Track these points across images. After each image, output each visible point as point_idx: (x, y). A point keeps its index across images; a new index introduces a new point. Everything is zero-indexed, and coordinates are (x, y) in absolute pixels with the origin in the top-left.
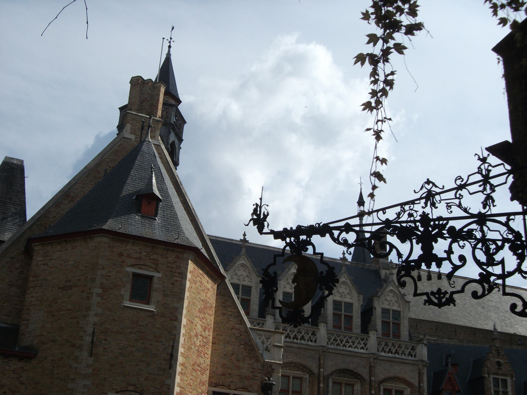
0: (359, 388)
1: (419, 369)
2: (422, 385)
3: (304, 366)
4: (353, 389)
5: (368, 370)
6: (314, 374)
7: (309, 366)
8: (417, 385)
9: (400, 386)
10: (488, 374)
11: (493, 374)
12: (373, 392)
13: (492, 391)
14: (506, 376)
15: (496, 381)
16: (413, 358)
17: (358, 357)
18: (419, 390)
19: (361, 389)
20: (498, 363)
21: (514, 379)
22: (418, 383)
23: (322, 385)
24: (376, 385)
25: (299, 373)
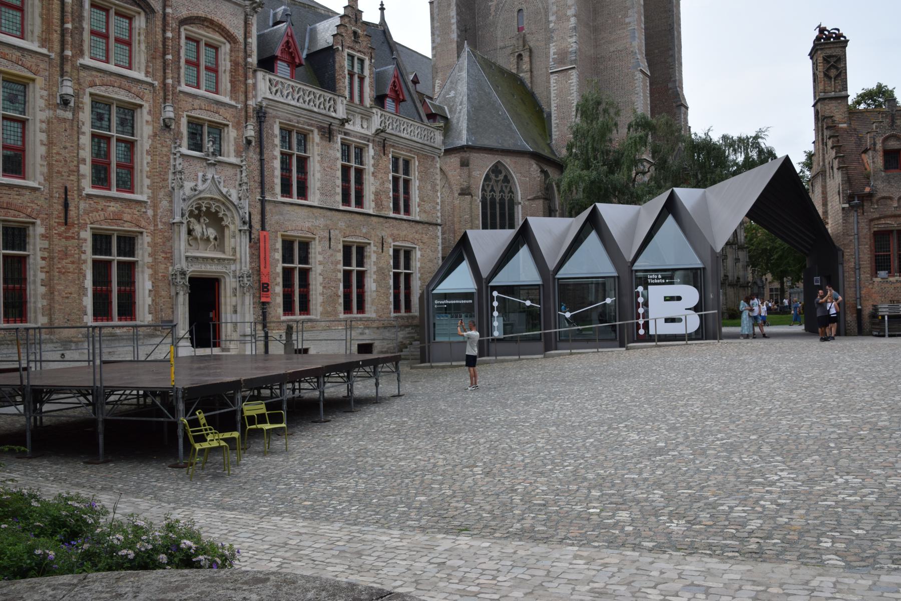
0: (143, 25)
1: (246, 15)
2: (249, 40)
4: (130, 24)
8: (241, 38)
10: (342, 46)
11: (349, 48)
12: (169, 34)
13: (346, 72)
14: (365, 54)
15: (351, 57)
19: (147, 26)
20: (355, 33)
22: (243, 36)
24: (174, 25)
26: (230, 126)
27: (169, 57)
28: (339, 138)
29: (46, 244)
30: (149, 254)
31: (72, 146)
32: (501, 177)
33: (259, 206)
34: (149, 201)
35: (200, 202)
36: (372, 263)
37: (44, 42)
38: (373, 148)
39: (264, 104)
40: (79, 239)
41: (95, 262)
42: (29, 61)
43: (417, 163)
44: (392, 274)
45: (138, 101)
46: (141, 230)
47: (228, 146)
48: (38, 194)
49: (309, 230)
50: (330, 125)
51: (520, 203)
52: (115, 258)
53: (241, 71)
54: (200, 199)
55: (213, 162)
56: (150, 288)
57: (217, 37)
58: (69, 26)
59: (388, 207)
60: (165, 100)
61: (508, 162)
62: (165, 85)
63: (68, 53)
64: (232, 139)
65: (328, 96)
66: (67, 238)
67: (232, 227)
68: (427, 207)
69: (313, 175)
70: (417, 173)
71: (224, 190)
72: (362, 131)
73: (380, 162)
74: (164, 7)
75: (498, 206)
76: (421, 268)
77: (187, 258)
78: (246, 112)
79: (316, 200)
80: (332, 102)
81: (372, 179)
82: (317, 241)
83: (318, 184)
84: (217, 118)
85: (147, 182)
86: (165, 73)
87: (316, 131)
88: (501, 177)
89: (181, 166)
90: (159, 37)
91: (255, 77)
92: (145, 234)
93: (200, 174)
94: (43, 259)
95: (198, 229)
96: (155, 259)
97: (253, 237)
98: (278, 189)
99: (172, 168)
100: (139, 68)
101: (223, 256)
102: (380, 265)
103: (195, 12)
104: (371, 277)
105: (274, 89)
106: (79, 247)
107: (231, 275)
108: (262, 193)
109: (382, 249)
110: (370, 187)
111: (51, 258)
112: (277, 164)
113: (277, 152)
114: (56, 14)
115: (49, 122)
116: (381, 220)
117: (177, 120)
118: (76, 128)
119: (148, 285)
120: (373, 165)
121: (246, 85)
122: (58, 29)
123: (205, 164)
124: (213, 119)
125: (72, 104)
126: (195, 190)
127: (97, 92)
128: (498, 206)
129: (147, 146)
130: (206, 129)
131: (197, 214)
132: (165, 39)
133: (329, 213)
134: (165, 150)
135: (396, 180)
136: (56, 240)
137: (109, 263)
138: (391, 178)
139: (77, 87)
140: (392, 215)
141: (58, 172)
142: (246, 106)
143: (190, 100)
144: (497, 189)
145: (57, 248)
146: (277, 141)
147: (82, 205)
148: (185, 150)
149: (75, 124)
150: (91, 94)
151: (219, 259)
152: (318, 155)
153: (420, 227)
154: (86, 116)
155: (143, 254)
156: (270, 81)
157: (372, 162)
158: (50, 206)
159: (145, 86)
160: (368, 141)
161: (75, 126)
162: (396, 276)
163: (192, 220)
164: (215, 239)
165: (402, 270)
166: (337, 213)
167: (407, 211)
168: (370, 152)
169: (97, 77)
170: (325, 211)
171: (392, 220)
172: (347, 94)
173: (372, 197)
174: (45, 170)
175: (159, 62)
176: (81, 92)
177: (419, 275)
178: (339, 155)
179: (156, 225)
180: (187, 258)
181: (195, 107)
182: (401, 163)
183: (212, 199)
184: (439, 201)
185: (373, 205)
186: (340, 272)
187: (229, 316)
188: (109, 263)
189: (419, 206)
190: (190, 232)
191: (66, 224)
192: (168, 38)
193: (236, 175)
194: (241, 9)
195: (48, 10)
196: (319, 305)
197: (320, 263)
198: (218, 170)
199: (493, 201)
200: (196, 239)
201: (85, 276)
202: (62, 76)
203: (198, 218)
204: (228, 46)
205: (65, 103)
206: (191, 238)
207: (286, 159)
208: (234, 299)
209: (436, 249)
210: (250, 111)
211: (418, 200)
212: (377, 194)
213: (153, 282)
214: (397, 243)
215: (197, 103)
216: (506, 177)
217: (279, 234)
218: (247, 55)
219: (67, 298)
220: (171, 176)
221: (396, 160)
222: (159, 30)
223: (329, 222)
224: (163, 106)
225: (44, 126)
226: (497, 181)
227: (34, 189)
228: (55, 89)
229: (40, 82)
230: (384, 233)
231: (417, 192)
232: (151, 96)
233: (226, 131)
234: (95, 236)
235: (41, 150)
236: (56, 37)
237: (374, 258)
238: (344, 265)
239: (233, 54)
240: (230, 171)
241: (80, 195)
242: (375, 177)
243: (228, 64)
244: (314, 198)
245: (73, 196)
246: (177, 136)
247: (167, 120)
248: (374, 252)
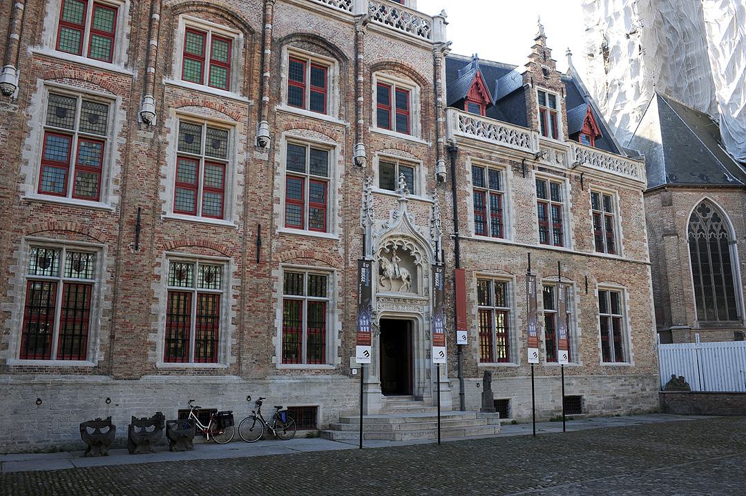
0: (337, 73)
1: (435, 58)
2: (439, 81)
3: (234, 16)
5: (352, 43)
6: (253, 32)
7: (244, 17)
8: (430, 80)
9: (405, 82)
11: (539, 84)
12: (361, 78)
14: (556, 90)
15: (542, 94)
16: (426, 39)
17: (335, 18)
18: (435, 90)
20: (544, 70)
21: (565, 96)
23: (268, 52)
25: (225, 29)
26: (422, 164)
27: (361, 99)
28: (533, 173)
29: (237, 282)
30: (340, 294)
31: (266, 186)
32: (710, 215)
33: (452, 243)
34: (340, 239)
35: (391, 240)
36: (576, 305)
37: (246, 91)
38: (570, 183)
39: (455, 141)
40: (270, 277)
41: (285, 301)
43: (619, 198)
44: (598, 317)
46: (332, 268)
47: (420, 184)
48: (233, 232)
49: (506, 269)
50: (524, 160)
51: (735, 242)
52: (306, 298)
53: (431, 111)
54: (391, 237)
55: (404, 199)
56: (341, 329)
57: (408, 80)
58: (268, 74)
59: (591, 245)
60: (357, 139)
61: (716, 198)
62: (357, 125)
63: (266, 99)
64: (423, 176)
65: (520, 130)
66: (258, 276)
67: (424, 265)
68: (634, 244)
69: (508, 212)
70: (619, 208)
71: (416, 228)
72: (558, 166)
73: (579, 197)
74: (357, 53)
75: (709, 246)
76: (632, 311)
77: (378, 298)
78: (438, 150)
79: (513, 238)
80: (524, 137)
81: (571, 214)
82: (515, 281)
83: (513, 222)
84: (409, 157)
85: (339, 220)
86: (357, 114)
87: (509, 167)
88: (710, 215)
89: (372, 204)
90: (352, 82)
91: (445, 115)
92: (336, 273)
93: (391, 212)
94: (235, 297)
95: (390, 268)
96: (346, 298)
97: (446, 275)
98: (471, 226)
99: (363, 205)
100: (333, 112)
101: (413, 296)
102: (584, 308)
103: (385, 58)
104: (575, 321)
105: (465, 126)
106: (270, 285)
107: (424, 317)
108: (456, 230)
109: (587, 290)
110: (570, 224)
111: (242, 296)
112: (470, 201)
113: (470, 189)
114: (257, 66)
115: (247, 164)
116: (584, 258)
117: (369, 161)
118: (271, 169)
119: (338, 326)
120: (571, 201)
121: (437, 123)
122: (258, 78)
123: (396, 202)
124: (404, 158)
125: (268, 146)
126: (387, 228)
127: (293, 135)
128: (709, 246)
129: (339, 185)
130: (397, 168)
131: (391, 251)
132: (357, 82)
134: (357, 187)
135: (597, 217)
136: (248, 279)
137: (301, 301)
138: (591, 214)
139: (273, 130)
140: (595, 253)
141: (253, 211)
142: (437, 143)
143: (382, 140)
144: (706, 228)
145: (248, 286)
146: (469, 177)
147: (275, 243)
148: (375, 187)
149: (271, 164)
151: (411, 300)
152: (513, 191)
153: (626, 266)
154: (282, 157)
155: (334, 293)
157: (570, 197)
158: (244, 244)
159: (339, 128)
160: (565, 176)
161: (271, 166)
162: (604, 320)
163: (384, 258)
164: (408, 279)
165: (609, 314)
167: (611, 250)
168: (567, 189)
169: (292, 120)
171: (595, 259)
172: (539, 128)
173: (572, 234)
174: (241, 209)
175: (351, 106)
176: (277, 135)
177: (629, 319)
178: (534, 190)
179: (347, 264)
180: (378, 298)
181: (386, 146)
182: (601, 198)
183: (403, 237)
184: (646, 237)
185: (574, 242)
187: (421, 360)
188: (301, 301)
189: (623, 244)
190: (382, 272)
191: (258, 262)
192: (360, 82)
193: (428, 212)
194: (430, 54)
195: (250, 62)
196: (519, 351)
198: (410, 208)
199: (702, 239)
200: (388, 278)
201: (275, 316)
202: (260, 120)
203: (390, 256)
204: (418, 88)
206: (383, 278)
207: (479, 196)
208: (427, 342)
209: (647, 290)
210: (442, 147)
211: (622, 236)
212: (577, 230)
213: (343, 323)
214: (602, 284)
216: (715, 214)
218: (437, 94)
219: (256, 337)
220: (362, 214)
221: (595, 196)
222: (351, 76)
224: (355, 146)
225: (242, 168)
226: (706, 221)
227: (230, 228)
228: (253, 132)
229: (240, 127)
230: (587, 273)
231: (621, 228)
232: (343, 137)
233: (417, 170)
234: (287, 274)
235: (239, 191)
236: (255, 86)
237: (577, 299)
238: (545, 309)
239: (423, 95)
240: (422, 209)
241: (273, 234)
242: (574, 213)
243: (419, 106)
244: (511, 236)
245: (266, 235)
246: (371, 172)
247: (358, 159)
248: (578, 293)
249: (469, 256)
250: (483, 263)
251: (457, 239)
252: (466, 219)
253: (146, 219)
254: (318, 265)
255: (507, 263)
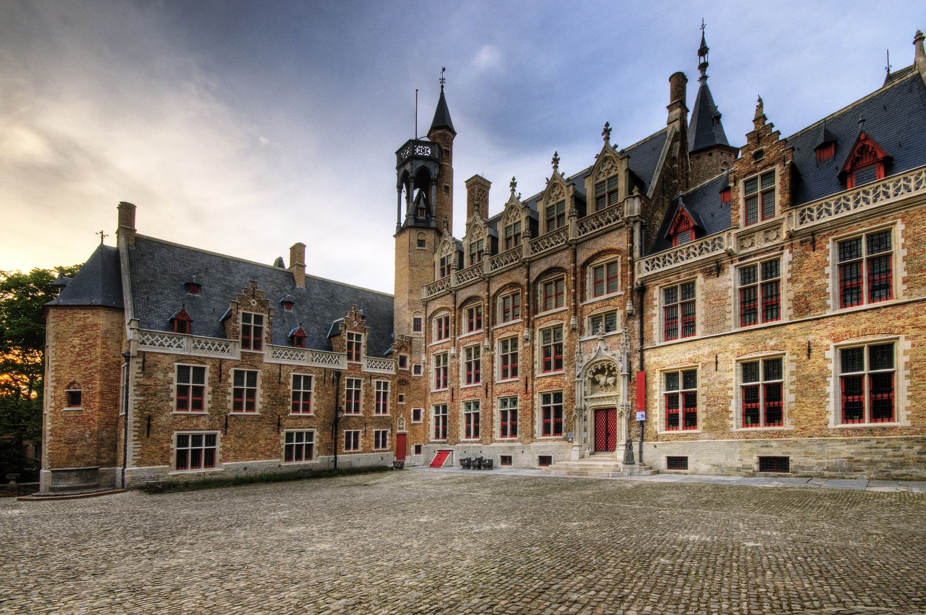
33: (638, 355)
42: (516, 327)
45: (561, 322)
49: (690, 359)
54: (596, 362)
57: (612, 256)
83: (703, 319)
84: (609, 309)
133: (717, 340)
150: (540, 330)
156: (647, 262)
166: (727, 337)
170: (710, 340)
186: (732, 389)
197: (703, 386)
205: (527, 340)
215: (594, 307)
217: (657, 371)
223: (716, 348)
230: (811, 338)
249: (653, 360)
250: (667, 362)
251: (642, 351)
252: (651, 334)
253: (489, 386)
254: (555, 389)
255: (691, 356)
